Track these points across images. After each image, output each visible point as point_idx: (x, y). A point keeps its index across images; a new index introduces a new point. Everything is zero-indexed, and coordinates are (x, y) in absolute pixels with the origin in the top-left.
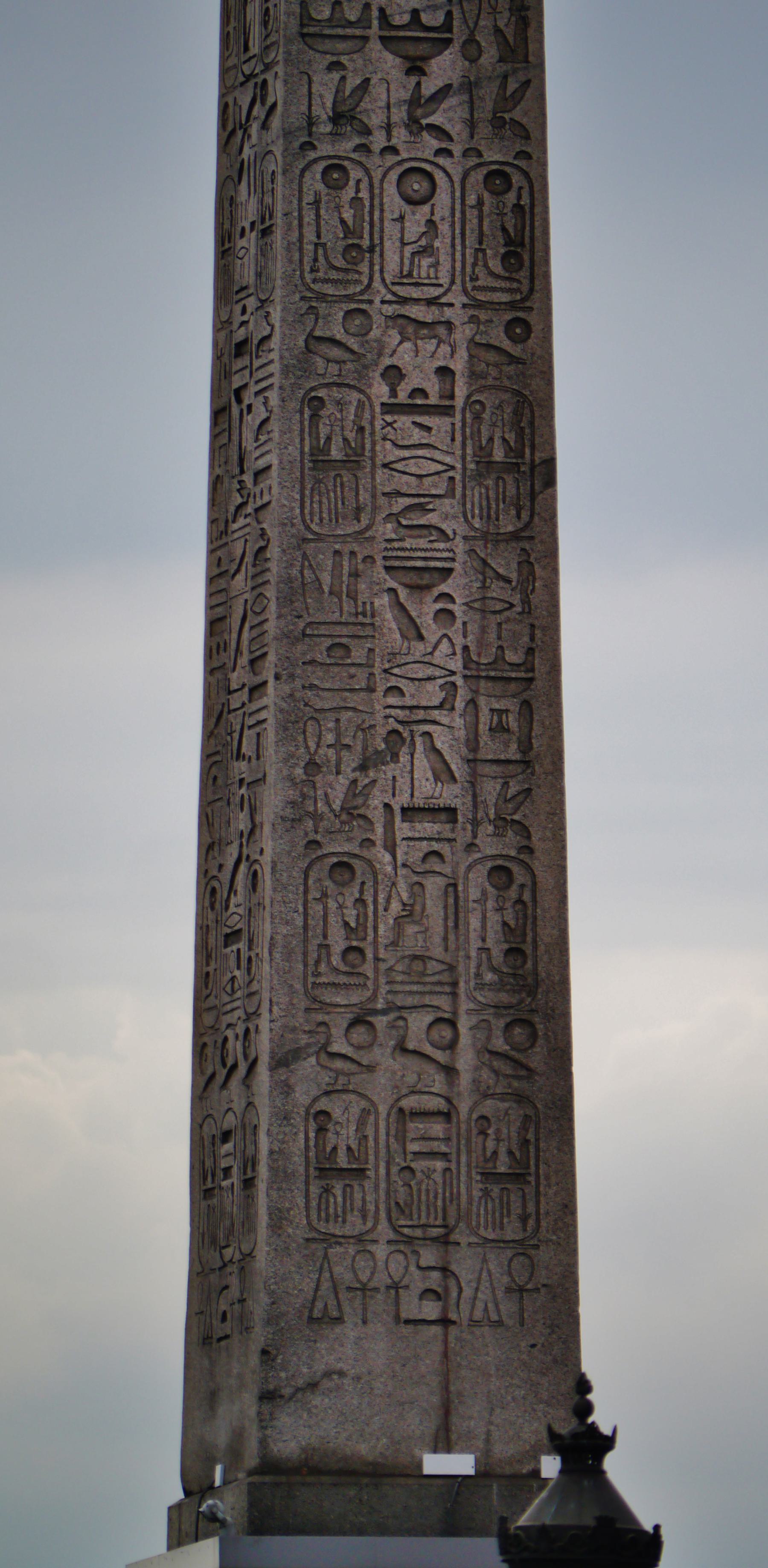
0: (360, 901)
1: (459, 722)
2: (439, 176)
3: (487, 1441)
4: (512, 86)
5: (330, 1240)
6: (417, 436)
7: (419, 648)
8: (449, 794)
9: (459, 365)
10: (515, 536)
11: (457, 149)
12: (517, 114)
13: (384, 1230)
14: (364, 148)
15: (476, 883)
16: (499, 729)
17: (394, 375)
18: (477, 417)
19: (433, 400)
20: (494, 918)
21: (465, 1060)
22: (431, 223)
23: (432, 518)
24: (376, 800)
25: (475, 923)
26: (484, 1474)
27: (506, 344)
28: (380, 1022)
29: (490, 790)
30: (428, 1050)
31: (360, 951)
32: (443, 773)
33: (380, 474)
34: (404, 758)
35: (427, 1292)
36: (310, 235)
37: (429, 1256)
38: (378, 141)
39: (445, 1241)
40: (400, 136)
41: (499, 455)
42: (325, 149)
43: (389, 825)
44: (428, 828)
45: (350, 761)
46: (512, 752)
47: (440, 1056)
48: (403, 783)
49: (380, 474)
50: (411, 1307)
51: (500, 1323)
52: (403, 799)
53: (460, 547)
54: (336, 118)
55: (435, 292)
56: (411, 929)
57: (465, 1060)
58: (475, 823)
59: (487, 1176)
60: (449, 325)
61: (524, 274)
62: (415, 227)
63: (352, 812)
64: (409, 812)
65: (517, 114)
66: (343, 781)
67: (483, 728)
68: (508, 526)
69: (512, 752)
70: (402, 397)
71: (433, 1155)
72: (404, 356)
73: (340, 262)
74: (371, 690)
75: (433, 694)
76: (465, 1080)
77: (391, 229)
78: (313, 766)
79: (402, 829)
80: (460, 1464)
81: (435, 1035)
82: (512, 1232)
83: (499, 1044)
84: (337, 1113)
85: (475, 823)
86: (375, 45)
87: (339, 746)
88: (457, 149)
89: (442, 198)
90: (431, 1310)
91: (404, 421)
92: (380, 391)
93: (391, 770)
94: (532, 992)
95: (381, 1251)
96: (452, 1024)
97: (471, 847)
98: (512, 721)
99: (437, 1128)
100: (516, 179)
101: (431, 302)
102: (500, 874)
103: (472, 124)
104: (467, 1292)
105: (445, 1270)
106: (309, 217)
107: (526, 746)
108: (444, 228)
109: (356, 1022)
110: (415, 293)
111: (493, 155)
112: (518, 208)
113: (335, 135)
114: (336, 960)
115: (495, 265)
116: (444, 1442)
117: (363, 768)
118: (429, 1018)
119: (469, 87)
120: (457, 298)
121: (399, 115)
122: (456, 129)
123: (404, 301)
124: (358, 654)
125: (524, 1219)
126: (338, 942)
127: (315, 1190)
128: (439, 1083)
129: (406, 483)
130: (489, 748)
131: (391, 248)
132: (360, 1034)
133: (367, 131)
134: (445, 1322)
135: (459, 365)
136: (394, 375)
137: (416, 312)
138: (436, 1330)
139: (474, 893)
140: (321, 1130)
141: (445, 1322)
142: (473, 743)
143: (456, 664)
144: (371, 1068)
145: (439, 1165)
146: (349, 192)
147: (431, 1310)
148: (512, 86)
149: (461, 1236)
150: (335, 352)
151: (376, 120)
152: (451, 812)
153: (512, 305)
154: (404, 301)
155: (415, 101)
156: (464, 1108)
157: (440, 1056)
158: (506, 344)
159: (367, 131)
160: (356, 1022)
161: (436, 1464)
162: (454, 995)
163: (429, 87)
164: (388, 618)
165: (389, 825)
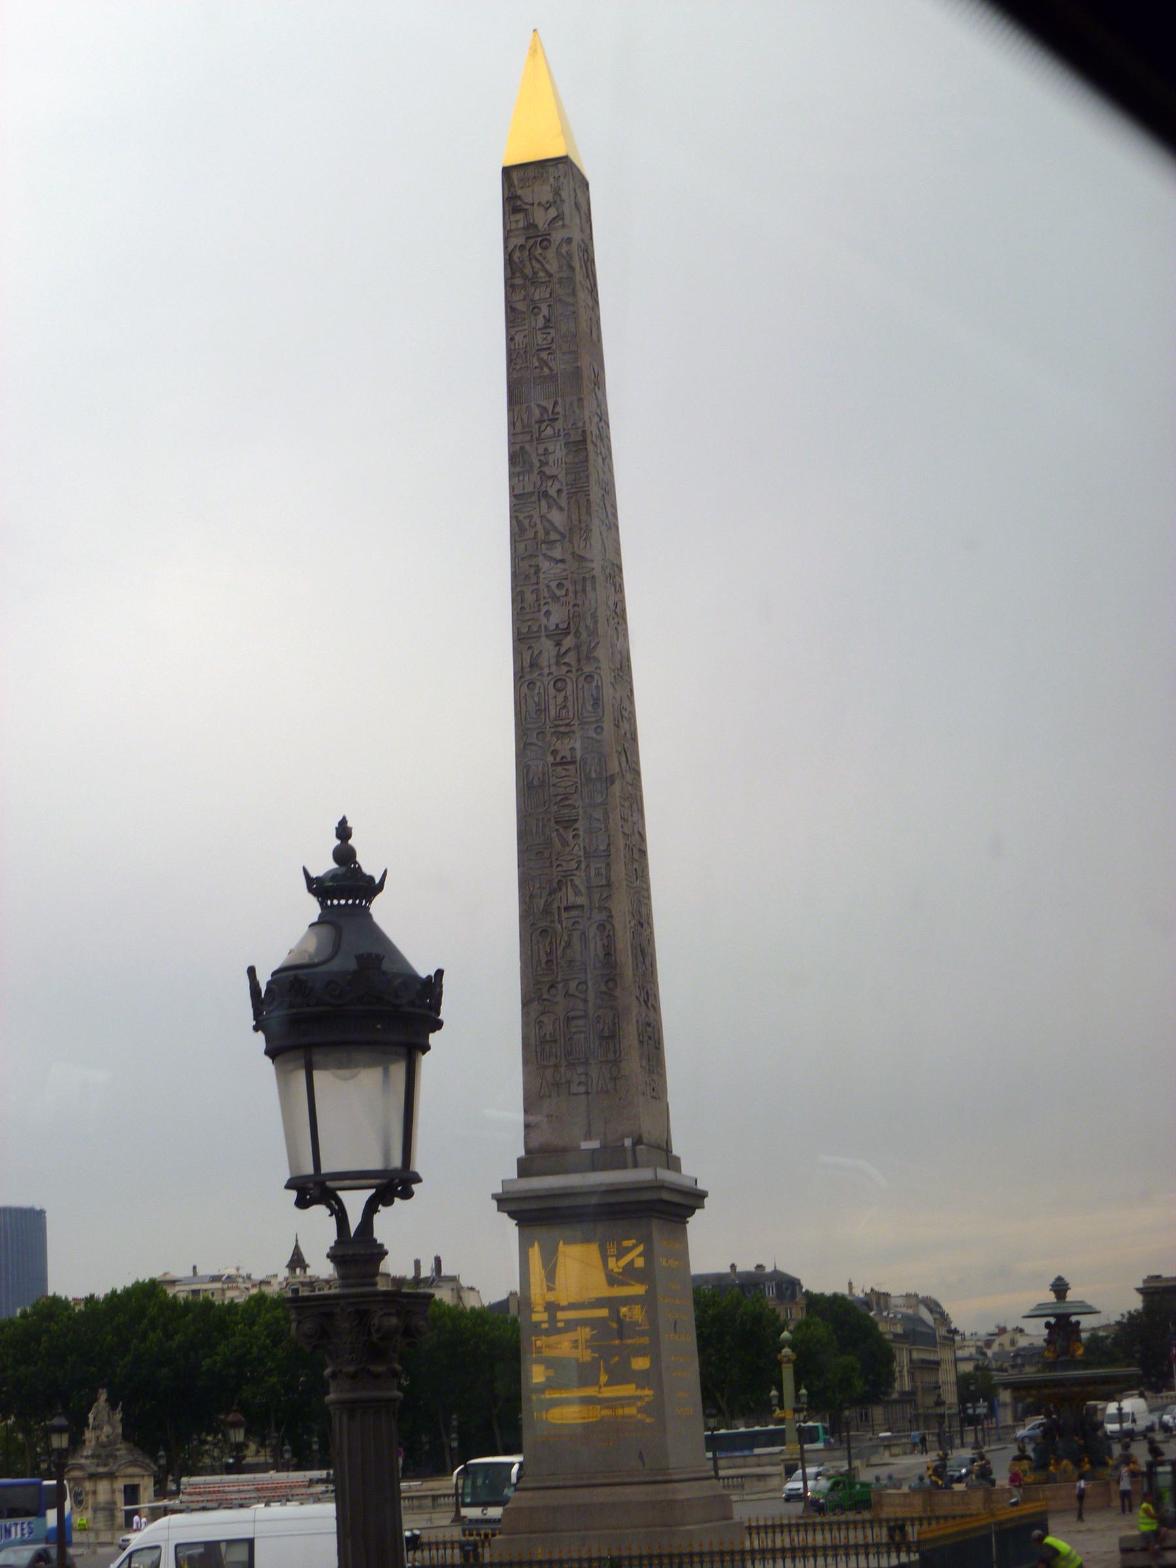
0: (551, 943)
1: (583, 874)
2: (568, 681)
3: (605, 1134)
4: (593, 645)
5: (545, 1067)
6: (564, 773)
7: (568, 849)
8: (581, 900)
9: (578, 745)
10: (602, 804)
11: (574, 670)
12: (595, 654)
13: (564, 1063)
14: (541, 675)
15: (592, 931)
16: (598, 874)
17: (554, 753)
18: (585, 763)
19: (569, 759)
20: (599, 945)
21: (591, 996)
22: (565, 697)
23: (570, 802)
24: (555, 906)
25: (592, 946)
26: (603, 1147)
27: (595, 736)
28: (560, 986)
29: (596, 897)
30: (577, 994)
31: (551, 961)
32: (577, 893)
33: (552, 789)
34: (564, 889)
35: (579, 1084)
36: (523, 707)
37: (580, 1070)
38: (546, 671)
39: (586, 1063)
40: (553, 668)
41: (593, 775)
42: (528, 677)
43: (559, 915)
44: (574, 913)
45: (545, 893)
46: (604, 882)
47: (582, 996)
48: (564, 898)
49: (552, 789)
50: (575, 1089)
51: (607, 1091)
52: (564, 904)
53: (581, 811)
54: (531, 666)
55: (567, 721)
56: (568, 951)
57: (591, 996)
58: (591, 910)
59: (602, 1038)
60: (573, 732)
61: (600, 710)
62: (560, 700)
63: (547, 911)
64: (567, 909)
65: (595, 654)
66: (543, 901)
67: (592, 874)
68: (599, 800)
69: (604, 882)
70: (558, 759)
71: (580, 1032)
72: (558, 746)
73: (534, 716)
74: (551, 866)
75: (574, 865)
76: (591, 1004)
77: (552, 702)
78: (531, 896)
79: (564, 915)
80: (594, 1144)
81: (580, 987)
82: (611, 1057)
83: (603, 988)
84: (546, 1021)
85: (591, 910)
86: (544, 639)
87: (541, 888)
88: (574, 670)
89: (569, 687)
90: (582, 1089)
91: (559, 769)
92: (550, 759)
93: (558, 895)
94: (615, 968)
95: (563, 1070)
96: (585, 983)
97: (590, 918)
98: (603, 871)
99: (581, 1022)
100: (596, 677)
101: (567, 725)
102: (602, 926)
103: (579, 661)
104: (595, 1081)
105: (587, 1074)
106: (523, 702)
107: (608, 879)
108: (570, 698)
109: (552, 986)
110: (561, 723)
111: (587, 669)
112: (597, 686)
113: (531, 672)
114: (543, 965)
115: (590, 708)
116: (588, 1136)
117: (550, 894)
118: (576, 982)
119: (578, 647)
120: (575, 722)
121: (553, 661)
122: (573, 663)
123: (558, 726)
124: (547, 854)
125: (615, 1052)
126: (544, 959)
127: (539, 1049)
128: (581, 1005)
129: (561, 790)
130: (595, 881)
131: (552, 708)
132: (553, 991)
133: (542, 669)
134: (587, 1093)
135: (578, 745)
136: (554, 753)
137: (562, 729)
138: (583, 1096)
139: (591, 935)
140: (540, 1028)
141: (587, 1093)
142: (588, 880)
143: (582, 853)
144: (557, 1003)
145: (583, 1035)
146: (537, 691)
147: (582, 1089)
148: (593, 645)
149: (591, 1061)
150: (534, 748)
151: (545, 664)
152: (582, 906)
153: (597, 721)
154: (558, 726)
155: (559, 656)
156: (591, 1013)
157: (582, 996)
158: (595, 736)
159: (542, 669)
160: (552, 986)
161: (586, 1145)
162: (586, 973)
163: (563, 650)
164: (556, 841)
165: (559, 915)
